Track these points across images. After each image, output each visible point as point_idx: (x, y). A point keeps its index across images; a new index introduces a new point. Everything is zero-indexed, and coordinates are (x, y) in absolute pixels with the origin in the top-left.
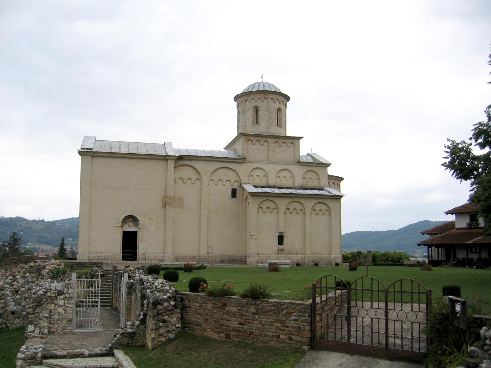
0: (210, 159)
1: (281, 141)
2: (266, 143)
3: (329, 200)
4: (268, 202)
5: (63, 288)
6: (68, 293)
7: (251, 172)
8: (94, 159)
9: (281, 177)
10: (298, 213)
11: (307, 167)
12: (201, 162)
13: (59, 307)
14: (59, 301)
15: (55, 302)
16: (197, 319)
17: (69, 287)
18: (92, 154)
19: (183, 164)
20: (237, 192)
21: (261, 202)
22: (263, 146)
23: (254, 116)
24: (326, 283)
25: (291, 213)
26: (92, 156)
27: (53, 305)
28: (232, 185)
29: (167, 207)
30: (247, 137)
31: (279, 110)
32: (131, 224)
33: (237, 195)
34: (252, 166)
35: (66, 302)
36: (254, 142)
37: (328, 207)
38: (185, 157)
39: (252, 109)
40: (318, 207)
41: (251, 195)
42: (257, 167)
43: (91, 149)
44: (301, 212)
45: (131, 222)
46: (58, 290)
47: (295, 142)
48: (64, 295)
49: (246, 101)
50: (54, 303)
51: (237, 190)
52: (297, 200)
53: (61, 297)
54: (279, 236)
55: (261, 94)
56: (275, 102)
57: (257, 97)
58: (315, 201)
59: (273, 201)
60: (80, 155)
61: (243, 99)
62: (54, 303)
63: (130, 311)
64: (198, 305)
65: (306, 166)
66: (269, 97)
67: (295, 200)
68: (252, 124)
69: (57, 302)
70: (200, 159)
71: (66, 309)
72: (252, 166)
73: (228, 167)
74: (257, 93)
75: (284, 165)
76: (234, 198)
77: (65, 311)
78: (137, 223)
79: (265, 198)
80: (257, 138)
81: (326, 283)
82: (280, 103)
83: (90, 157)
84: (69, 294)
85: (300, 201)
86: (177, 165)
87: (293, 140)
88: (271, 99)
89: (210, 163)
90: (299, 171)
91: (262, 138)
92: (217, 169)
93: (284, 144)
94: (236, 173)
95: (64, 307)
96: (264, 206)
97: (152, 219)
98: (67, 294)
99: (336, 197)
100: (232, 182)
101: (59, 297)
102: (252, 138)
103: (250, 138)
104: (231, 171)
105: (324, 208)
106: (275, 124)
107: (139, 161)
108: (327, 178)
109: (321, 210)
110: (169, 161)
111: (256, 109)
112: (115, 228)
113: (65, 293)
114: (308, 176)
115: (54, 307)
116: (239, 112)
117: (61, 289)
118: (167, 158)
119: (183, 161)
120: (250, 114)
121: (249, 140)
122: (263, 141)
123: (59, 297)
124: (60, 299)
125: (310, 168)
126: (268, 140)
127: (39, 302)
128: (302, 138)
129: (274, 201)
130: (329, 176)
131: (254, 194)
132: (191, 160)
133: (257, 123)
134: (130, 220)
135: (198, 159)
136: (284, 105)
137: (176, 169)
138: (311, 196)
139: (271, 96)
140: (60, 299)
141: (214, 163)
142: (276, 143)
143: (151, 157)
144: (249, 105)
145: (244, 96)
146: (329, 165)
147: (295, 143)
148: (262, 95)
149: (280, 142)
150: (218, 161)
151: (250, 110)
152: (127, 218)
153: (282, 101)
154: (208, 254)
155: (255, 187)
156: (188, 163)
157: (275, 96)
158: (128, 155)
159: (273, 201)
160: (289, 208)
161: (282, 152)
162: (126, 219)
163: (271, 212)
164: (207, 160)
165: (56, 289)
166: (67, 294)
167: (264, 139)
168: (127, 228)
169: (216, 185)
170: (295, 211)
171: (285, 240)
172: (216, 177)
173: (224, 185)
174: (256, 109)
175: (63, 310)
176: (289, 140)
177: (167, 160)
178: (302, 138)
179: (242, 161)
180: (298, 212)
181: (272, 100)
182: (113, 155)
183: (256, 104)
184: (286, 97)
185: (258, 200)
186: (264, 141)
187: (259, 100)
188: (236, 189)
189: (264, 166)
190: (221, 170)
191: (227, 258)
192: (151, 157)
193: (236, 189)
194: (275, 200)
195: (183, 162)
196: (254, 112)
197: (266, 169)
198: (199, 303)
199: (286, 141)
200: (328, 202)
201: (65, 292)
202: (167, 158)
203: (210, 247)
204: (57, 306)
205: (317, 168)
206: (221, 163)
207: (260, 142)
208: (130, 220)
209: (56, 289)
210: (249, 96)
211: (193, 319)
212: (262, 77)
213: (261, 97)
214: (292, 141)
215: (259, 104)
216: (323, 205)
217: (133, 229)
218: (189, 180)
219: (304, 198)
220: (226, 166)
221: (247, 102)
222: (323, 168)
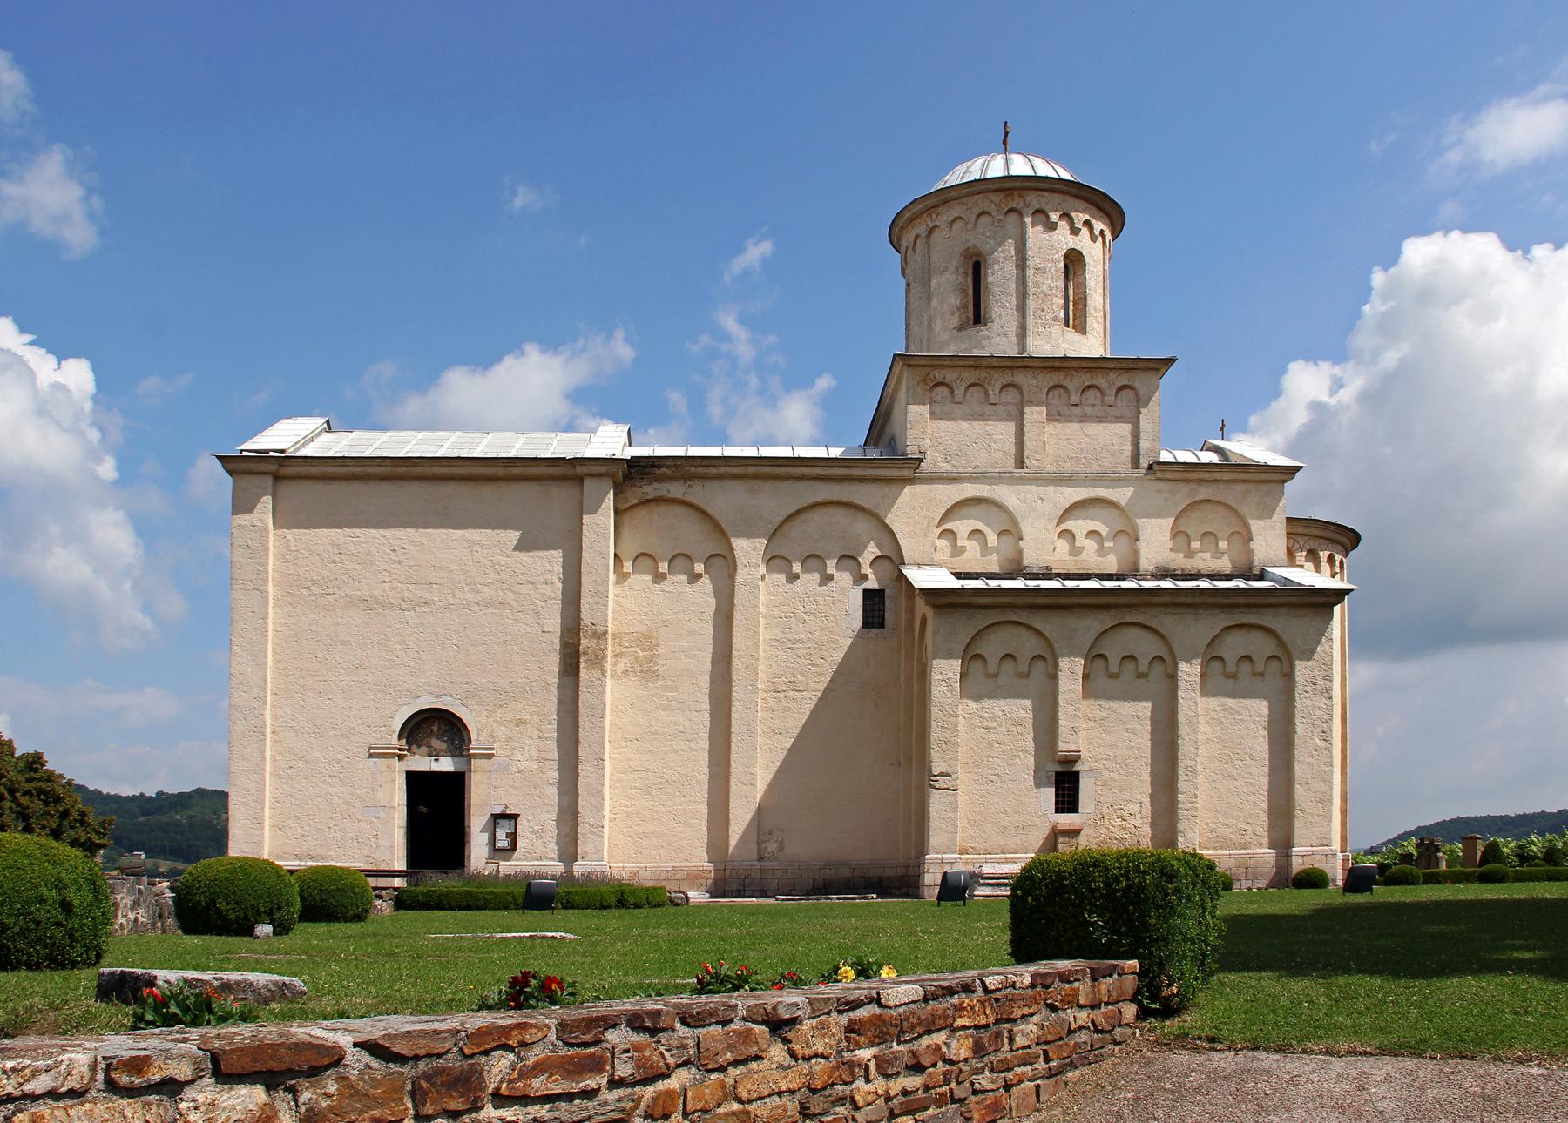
0: (768, 470)
1: (1074, 383)
2: (1011, 395)
3: (1283, 611)
4: (1012, 631)
7: (946, 517)
8: (287, 489)
12: (729, 484)
18: (273, 467)
19: (651, 496)
20: (887, 602)
23: (964, 291)
25: (1112, 676)
26: (277, 478)
29: (583, 673)
32: (437, 744)
34: (950, 494)
36: (959, 392)
37: (1281, 643)
38: (659, 467)
40: (1234, 646)
41: (935, 606)
43: (282, 451)
44: (1158, 669)
45: (440, 737)
47: (1140, 381)
49: (931, 231)
52: (1141, 619)
55: (993, 197)
57: (977, 211)
59: (1030, 627)
60: (231, 473)
66: (1027, 206)
67: (1128, 619)
68: (955, 321)
70: (722, 470)
72: (950, 494)
73: (845, 498)
74: (974, 194)
78: (462, 740)
80: (970, 376)
82: (1075, 231)
83: (269, 480)
86: (627, 500)
91: (992, 372)
93: (1091, 392)
96: (992, 648)
97: (521, 722)
99: (1314, 599)
102: (950, 376)
103: (938, 375)
104: (860, 516)
105: (1261, 646)
106: (1055, 319)
107: (464, 489)
109: (1247, 658)
110: (587, 482)
112: (373, 760)
116: (908, 285)
118: (580, 470)
119: (656, 485)
121: (936, 385)
122: (998, 385)
126: (1021, 378)
129: (1038, 626)
132: (687, 478)
134: (435, 728)
135: (713, 471)
136: (1094, 239)
137: (626, 518)
138: (1198, 600)
139: (1035, 200)
141: (786, 486)
142: (1057, 391)
143: (515, 471)
144: (948, 242)
147: (1137, 385)
149: (1070, 386)
150: (802, 478)
152: (424, 720)
153: (1087, 223)
154: (761, 859)
155: (958, 576)
156: (675, 489)
157: (1056, 198)
158: (418, 465)
159: (1030, 627)
160: (1103, 656)
162: (418, 725)
164: (755, 477)
167: (1000, 379)
168: (423, 763)
170: (1130, 666)
171: (1087, 790)
176: (1112, 376)
177: (579, 479)
178: (1171, 360)
179: (906, 473)
180: (1143, 668)
182: (358, 470)
184: (1106, 206)
186: (1003, 387)
187: (984, 219)
189: (1006, 495)
190: (816, 516)
191: (846, 872)
192: (515, 471)
194: (1038, 621)
195: (650, 490)
196: (966, 274)
199: (1100, 381)
202: (580, 470)
203: (770, 833)
206: (817, 484)
207: (986, 393)
208: (435, 728)
212: (1007, 134)
213: (992, 209)
214: (1123, 380)
217: (446, 765)
218: (682, 559)
219: (1170, 610)
221: (936, 237)
222: (1266, 487)
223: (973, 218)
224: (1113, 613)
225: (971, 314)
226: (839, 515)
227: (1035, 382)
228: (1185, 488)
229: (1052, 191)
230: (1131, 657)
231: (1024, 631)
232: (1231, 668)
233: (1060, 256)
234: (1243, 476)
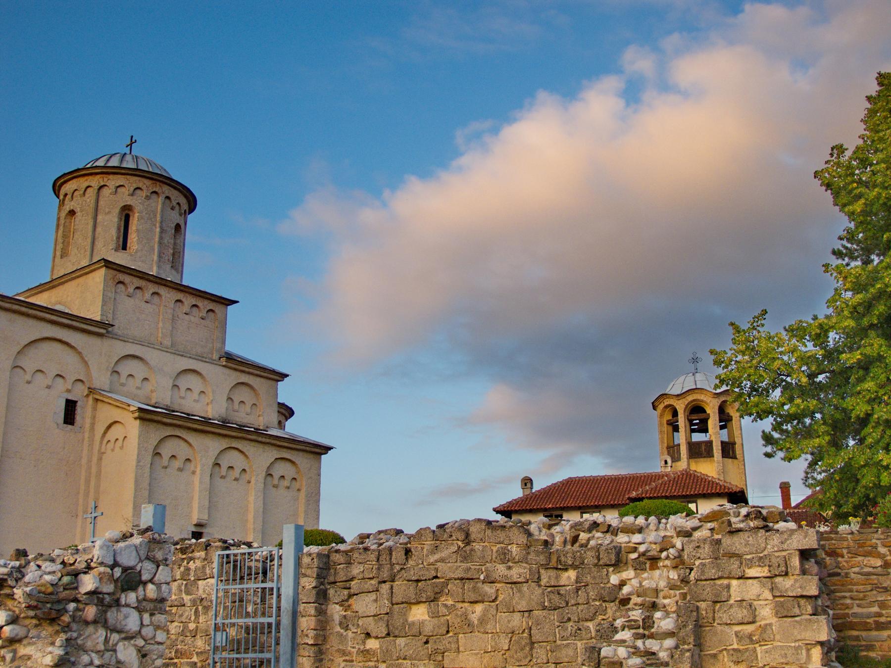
0: (24, 309)
2: (156, 299)
3: (301, 454)
5: (141, 561)
6: (153, 583)
9: (183, 389)
10: (236, 479)
11: (238, 374)
13: (125, 639)
14: (126, 617)
15: (111, 615)
16: (875, 609)
17: (159, 555)
21: (161, 441)
22: (149, 305)
23: (119, 229)
24: (750, 578)
27: (102, 633)
28: (68, 391)
30: (114, 272)
31: (178, 227)
33: (78, 418)
35: (146, 616)
39: (117, 210)
40: (282, 469)
42: (137, 354)
46: (125, 570)
47: (218, 308)
48: (141, 589)
50: (105, 625)
51: (79, 404)
52: (239, 446)
53: (131, 597)
54: (193, 532)
56: (173, 209)
57: (135, 186)
58: (275, 453)
61: (95, 182)
62: (106, 621)
63: (321, 660)
64: (879, 563)
65: (235, 370)
67: (233, 445)
68: (112, 245)
69: (121, 616)
71: (148, 647)
75: (191, 361)
76: (70, 426)
77: (144, 656)
79: (169, 431)
81: (750, 578)
84: (158, 586)
85: (244, 450)
87: (214, 304)
88: (168, 198)
89: (20, 321)
90: (223, 378)
91: (149, 283)
92: (32, 342)
94: (82, 358)
95: (140, 642)
98: (150, 586)
100: (71, 378)
101: (123, 596)
102: (127, 279)
103: (122, 277)
108: (276, 408)
109: (283, 477)
111: (126, 214)
113: (145, 583)
114: (243, 394)
115: (107, 640)
117: (131, 563)
120: (110, 222)
121: (118, 283)
122: (151, 292)
123: (123, 596)
124: (127, 605)
125: (244, 378)
126: (163, 291)
127: (54, 614)
128: (236, 302)
129: (191, 441)
130: (279, 403)
131: (149, 416)
133: (124, 248)
139: (167, 190)
140: (127, 605)
141: (31, 322)
145: (97, 174)
146: (284, 376)
148: (148, 182)
151: (109, 212)
157: (176, 193)
161: (193, 328)
163: (180, 470)
165: (115, 564)
166: (150, 586)
167: (152, 288)
169: (29, 382)
172: (30, 362)
173: (49, 387)
174: (126, 214)
175: (135, 653)
176: (206, 302)
178: (236, 302)
179: (103, 331)
181: (167, 201)
183: (129, 201)
185: (156, 434)
187: (138, 192)
188: (75, 402)
190: (46, 346)
193: (75, 402)
194: (191, 437)
197: (152, 363)
198: (880, 556)
200: (302, 460)
201: (145, 577)
204: (115, 637)
205: (258, 379)
206: (49, 326)
209: (115, 564)
210: (111, 177)
211: (856, 610)
213: (144, 187)
214: (211, 306)
215: (136, 202)
216: (288, 465)
220: (59, 337)
221: (106, 192)
223: (132, 189)
224: (227, 440)
225: (121, 243)
226: (58, 346)
227: (168, 296)
228: (235, 374)
229: (175, 188)
230: (232, 467)
231: (182, 443)
232: (276, 482)
233: (173, 226)
234: (262, 374)
